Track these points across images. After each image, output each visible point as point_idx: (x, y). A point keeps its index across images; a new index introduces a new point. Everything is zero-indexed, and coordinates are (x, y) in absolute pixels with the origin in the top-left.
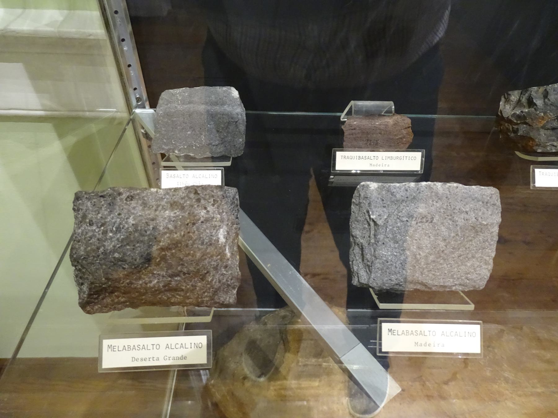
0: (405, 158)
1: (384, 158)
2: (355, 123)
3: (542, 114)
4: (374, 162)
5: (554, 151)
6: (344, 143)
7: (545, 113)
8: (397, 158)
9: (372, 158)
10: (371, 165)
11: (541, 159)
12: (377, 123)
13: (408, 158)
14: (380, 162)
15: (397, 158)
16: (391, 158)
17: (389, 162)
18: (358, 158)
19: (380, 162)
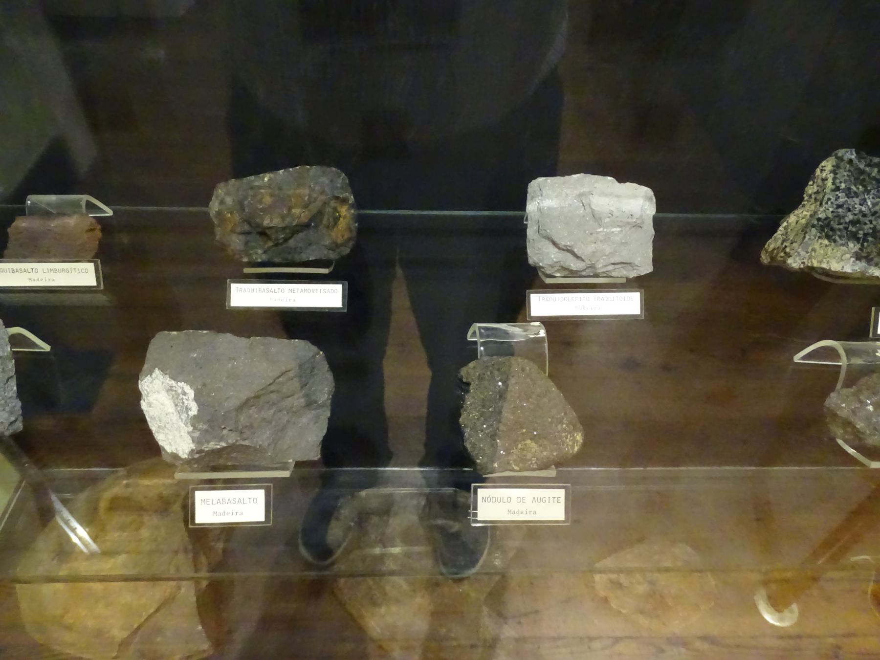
0: (73, 271)
1: (46, 270)
2: (24, 225)
3: (229, 215)
4: (33, 275)
5: (259, 260)
6: (6, 252)
7: (232, 213)
8: (63, 270)
9: (30, 270)
10: (30, 279)
11: (247, 270)
12: (52, 225)
13: (77, 271)
14: (40, 275)
15: (63, 270)
16: (55, 271)
17: (52, 275)
18: (11, 271)
19: (40, 275)
